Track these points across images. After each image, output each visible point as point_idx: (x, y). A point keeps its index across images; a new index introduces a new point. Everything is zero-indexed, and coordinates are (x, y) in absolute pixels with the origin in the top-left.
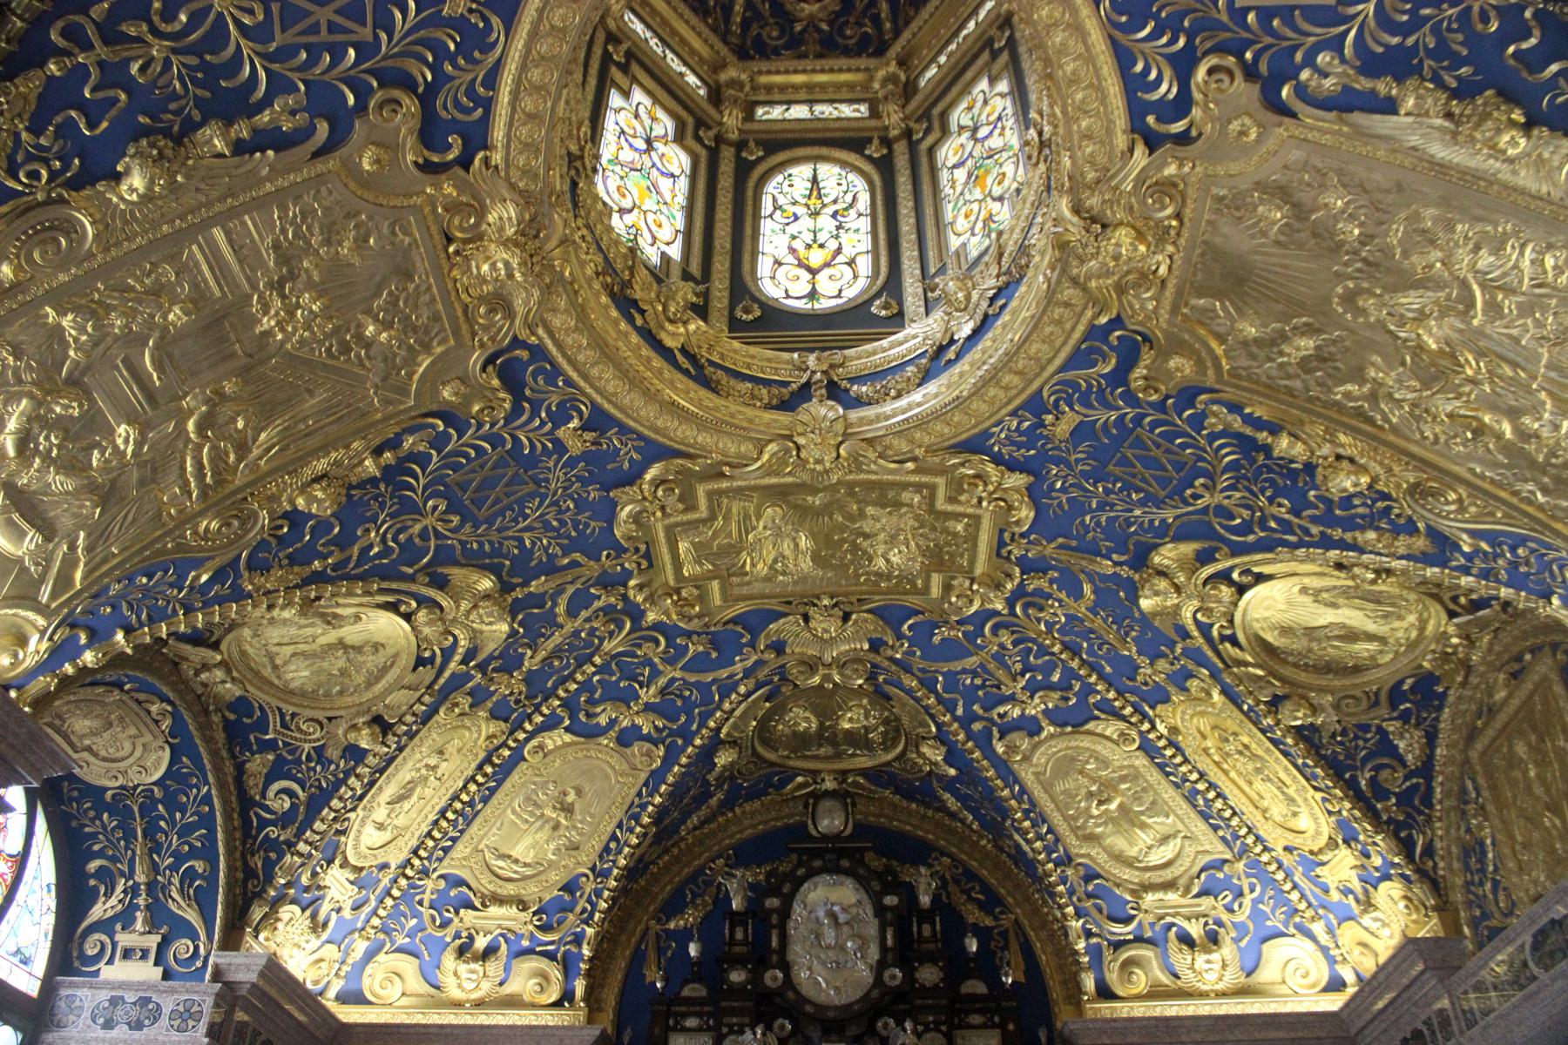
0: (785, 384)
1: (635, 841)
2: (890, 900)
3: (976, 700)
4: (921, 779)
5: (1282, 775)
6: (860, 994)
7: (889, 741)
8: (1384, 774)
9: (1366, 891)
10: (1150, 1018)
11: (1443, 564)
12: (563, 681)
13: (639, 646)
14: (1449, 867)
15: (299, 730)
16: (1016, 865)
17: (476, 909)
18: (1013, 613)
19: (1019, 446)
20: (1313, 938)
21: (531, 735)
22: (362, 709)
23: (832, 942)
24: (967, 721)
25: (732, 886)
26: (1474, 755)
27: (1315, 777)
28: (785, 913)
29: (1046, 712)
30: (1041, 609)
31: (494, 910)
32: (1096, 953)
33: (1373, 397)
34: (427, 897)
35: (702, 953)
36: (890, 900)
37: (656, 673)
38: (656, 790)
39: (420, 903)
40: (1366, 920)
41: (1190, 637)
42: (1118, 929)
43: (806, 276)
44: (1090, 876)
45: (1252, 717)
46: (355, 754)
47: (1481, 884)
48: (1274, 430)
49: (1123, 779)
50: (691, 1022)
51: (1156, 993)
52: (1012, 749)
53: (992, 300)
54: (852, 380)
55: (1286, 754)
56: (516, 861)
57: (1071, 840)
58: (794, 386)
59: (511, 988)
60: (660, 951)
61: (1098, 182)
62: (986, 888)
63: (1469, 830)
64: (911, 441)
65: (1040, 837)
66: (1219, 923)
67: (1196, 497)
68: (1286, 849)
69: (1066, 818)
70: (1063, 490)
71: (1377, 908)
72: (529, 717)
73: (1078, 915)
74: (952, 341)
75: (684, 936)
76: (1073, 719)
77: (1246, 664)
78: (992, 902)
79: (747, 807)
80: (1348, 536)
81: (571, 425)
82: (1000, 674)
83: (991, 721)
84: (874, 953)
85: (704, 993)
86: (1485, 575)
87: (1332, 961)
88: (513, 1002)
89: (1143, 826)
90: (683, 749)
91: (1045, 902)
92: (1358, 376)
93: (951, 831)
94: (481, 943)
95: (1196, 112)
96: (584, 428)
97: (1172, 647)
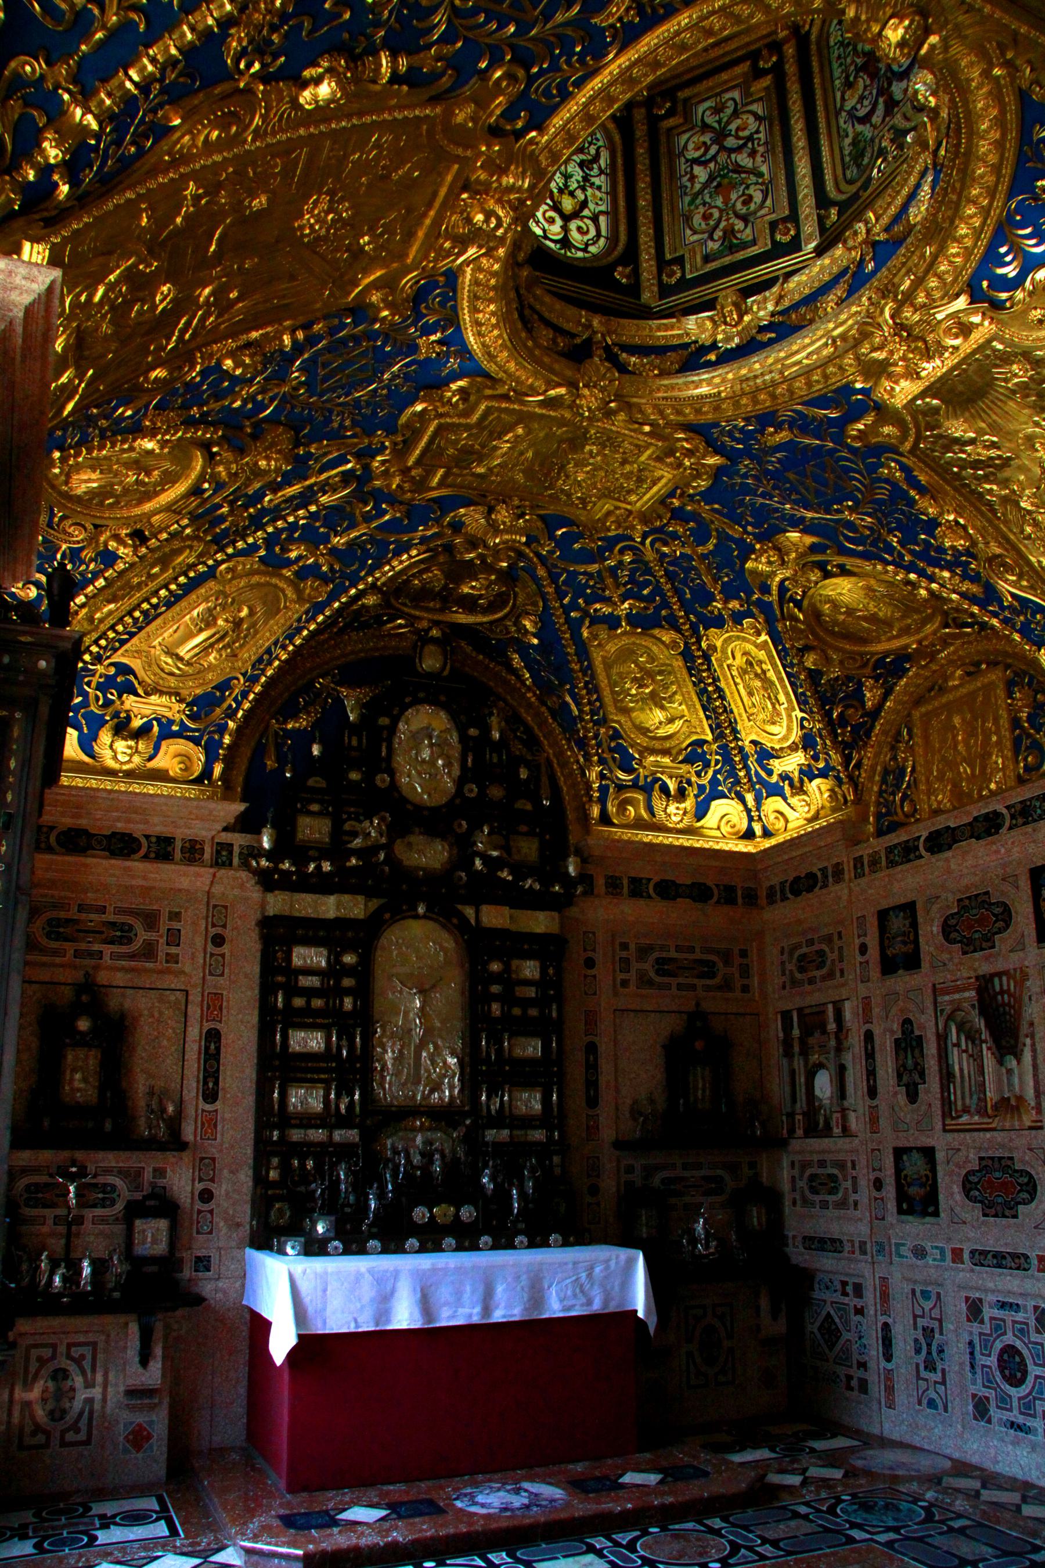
0: (573, 336)
1: (284, 657)
2: (473, 732)
3: (582, 594)
4: (498, 641)
5: (782, 698)
6: (444, 800)
7: (492, 607)
8: (851, 711)
9: (801, 781)
10: (633, 842)
11: (983, 606)
12: (274, 521)
13: (349, 503)
14: (871, 778)
15: (65, 532)
16: (554, 718)
17: (138, 695)
18: (643, 543)
19: (734, 439)
20: (742, 800)
21: (230, 557)
22: (126, 522)
23: (425, 757)
24: (566, 610)
25: (349, 704)
26: (916, 714)
27: (806, 703)
28: (393, 729)
29: (629, 616)
30: (666, 544)
31: (154, 699)
32: (604, 790)
33: (1005, 500)
34: (95, 680)
35: (322, 753)
36: (473, 732)
37: (352, 526)
38: (313, 619)
39: (89, 684)
40: (794, 801)
41: (770, 593)
42: (621, 775)
43: (559, 222)
44: (616, 735)
45: (783, 654)
46: (109, 558)
47: (894, 794)
48: (922, 490)
49: (660, 673)
50: (315, 807)
51: (640, 824)
52: (595, 637)
53: (762, 329)
54: (624, 348)
55: (791, 684)
56: (180, 659)
57: (611, 709)
58: (578, 341)
59: (161, 762)
60: (278, 747)
61: (924, 305)
62: (528, 730)
63: (894, 758)
64: (661, 413)
65: (590, 703)
66: (689, 782)
67: (838, 511)
68: (753, 742)
69: (613, 692)
70: (745, 476)
71: (805, 793)
72: (233, 543)
73: (602, 761)
74: (714, 346)
75: (304, 738)
76: (643, 622)
77: (797, 620)
78: (532, 742)
79: (354, 634)
80: (929, 570)
81: (433, 338)
82: (609, 581)
83: (586, 613)
84: (456, 771)
85: (323, 784)
86: (1005, 621)
87: (751, 819)
88: (160, 776)
89: (662, 708)
90: (346, 590)
91: (571, 749)
92: (1005, 483)
93: (506, 682)
94: (137, 723)
95: (1019, 295)
96: (439, 342)
97: (749, 593)
